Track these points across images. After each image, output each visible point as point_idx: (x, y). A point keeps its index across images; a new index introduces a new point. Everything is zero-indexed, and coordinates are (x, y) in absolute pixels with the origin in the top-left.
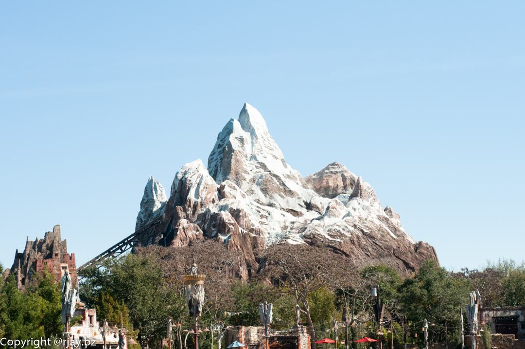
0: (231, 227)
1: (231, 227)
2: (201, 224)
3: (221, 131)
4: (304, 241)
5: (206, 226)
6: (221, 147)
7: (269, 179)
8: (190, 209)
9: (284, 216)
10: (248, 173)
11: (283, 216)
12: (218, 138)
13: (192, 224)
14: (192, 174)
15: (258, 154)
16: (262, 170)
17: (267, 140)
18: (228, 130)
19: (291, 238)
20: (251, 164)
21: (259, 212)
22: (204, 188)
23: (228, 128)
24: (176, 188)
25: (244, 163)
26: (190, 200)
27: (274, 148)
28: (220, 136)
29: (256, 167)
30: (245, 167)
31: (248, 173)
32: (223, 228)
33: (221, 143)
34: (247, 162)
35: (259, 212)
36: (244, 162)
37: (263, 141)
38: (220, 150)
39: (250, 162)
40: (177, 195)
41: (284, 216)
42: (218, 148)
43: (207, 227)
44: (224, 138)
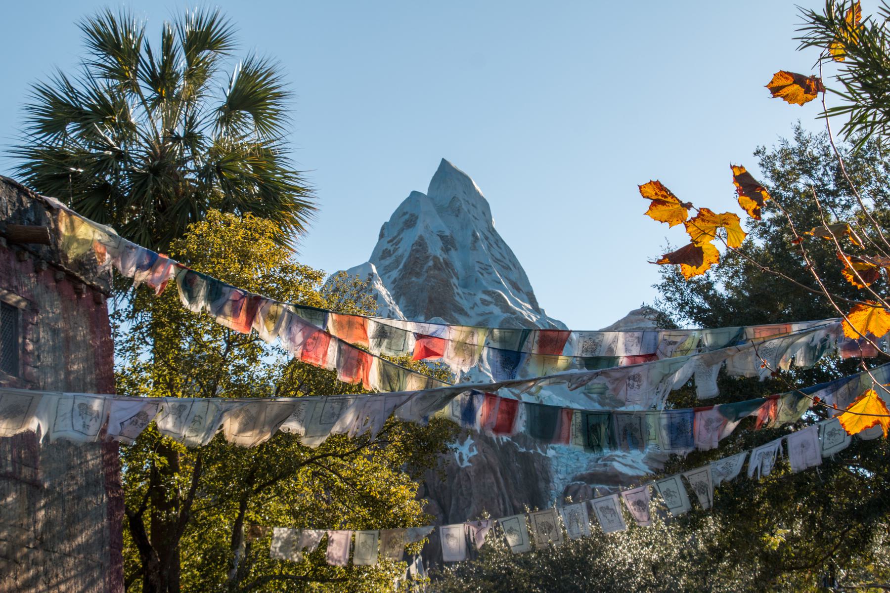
3: (388, 221)
4: (650, 469)
6: (390, 255)
10: (466, 314)
12: (382, 235)
15: (482, 274)
16: (496, 310)
17: (495, 246)
18: (407, 217)
19: (620, 460)
20: (470, 294)
23: (405, 214)
25: (456, 290)
27: (511, 266)
28: (386, 234)
30: (457, 298)
31: (466, 314)
33: (390, 247)
34: (460, 291)
36: (455, 288)
37: (488, 247)
38: (388, 261)
39: (466, 291)
42: (383, 257)
44: (399, 234)
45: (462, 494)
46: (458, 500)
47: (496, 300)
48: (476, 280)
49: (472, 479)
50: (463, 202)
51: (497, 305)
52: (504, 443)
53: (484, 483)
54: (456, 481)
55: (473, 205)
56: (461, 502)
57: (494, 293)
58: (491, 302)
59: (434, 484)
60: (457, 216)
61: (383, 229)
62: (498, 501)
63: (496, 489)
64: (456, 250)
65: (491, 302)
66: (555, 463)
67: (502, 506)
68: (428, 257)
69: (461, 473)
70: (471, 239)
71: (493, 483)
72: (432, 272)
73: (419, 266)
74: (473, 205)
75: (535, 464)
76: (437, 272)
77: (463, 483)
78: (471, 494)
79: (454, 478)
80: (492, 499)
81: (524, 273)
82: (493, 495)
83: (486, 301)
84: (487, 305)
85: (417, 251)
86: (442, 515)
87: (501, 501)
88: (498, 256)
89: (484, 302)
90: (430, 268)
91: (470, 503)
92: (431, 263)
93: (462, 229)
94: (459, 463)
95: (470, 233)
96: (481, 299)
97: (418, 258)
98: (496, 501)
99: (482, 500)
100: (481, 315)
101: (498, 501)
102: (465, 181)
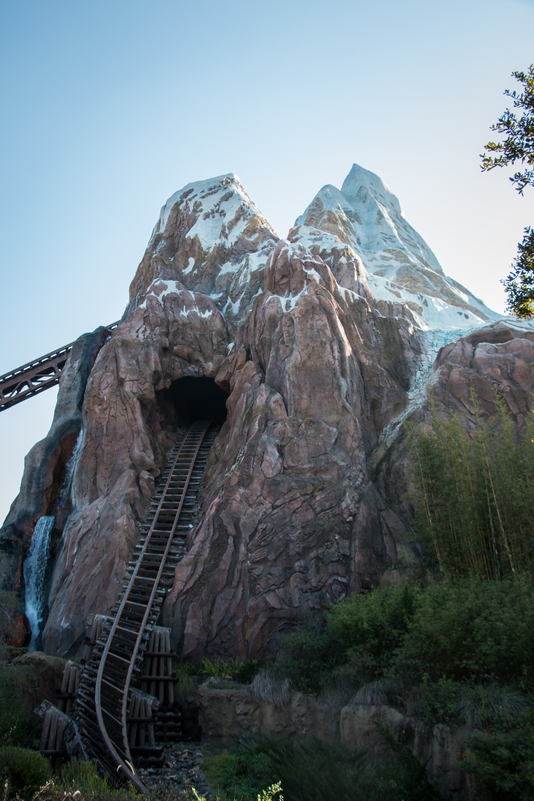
0: (312, 272)
1: (312, 272)
2: (223, 300)
5: (236, 307)
7: (415, 276)
8: (192, 261)
9: (467, 317)
11: (463, 315)
13: (190, 292)
14: (206, 192)
21: (399, 296)
22: (237, 219)
24: (162, 230)
26: (195, 241)
29: (383, 258)
32: (283, 277)
35: (399, 296)
40: (163, 244)
41: (467, 317)
43: (242, 308)
45: (283, 343)
46: (277, 350)
47: (396, 256)
48: (378, 244)
49: (296, 321)
50: (369, 190)
51: (397, 260)
52: (355, 300)
53: (312, 325)
54: (277, 330)
55: (380, 195)
56: (281, 351)
57: (395, 251)
58: (391, 258)
59: (255, 342)
60: (364, 202)
61: (297, 220)
62: (332, 348)
63: (328, 332)
64: (361, 224)
65: (391, 258)
66: (430, 337)
67: (336, 354)
68: (323, 213)
69: (284, 319)
70: (375, 217)
71: (325, 325)
72: (326, 224)
73: (314, 222)
74: (380, 195)
75: (400, 331)
76: (331, 225)
77: (285, 328)
78: (293, 341)
79: (276, 326)
80: (323, 344)
81: (434, 255)
82: (324, 340)
83: (385, 257)
84: (387, 260)
85: (313, 210)
86: (260, 375)
87: (336, 347)
88: (407, 237)
89: (383, 258)
90: (324, 221)
91: (292, 350)
92: (325, 217)
93: (369, 211)
94: (284, 311)
95: (375, 213)
96: (381, 256)
97: (313, 215)
98: (328, 347)
99: (308, 345)
100: (380, 267)
101: (332, 348)
102: (375, 179)
